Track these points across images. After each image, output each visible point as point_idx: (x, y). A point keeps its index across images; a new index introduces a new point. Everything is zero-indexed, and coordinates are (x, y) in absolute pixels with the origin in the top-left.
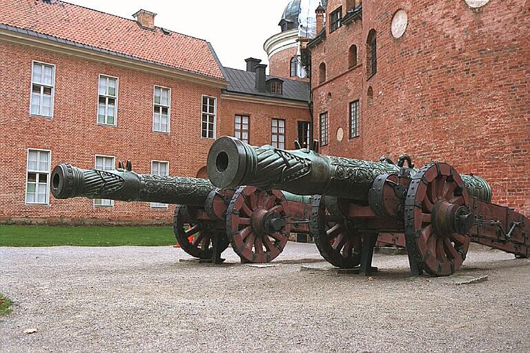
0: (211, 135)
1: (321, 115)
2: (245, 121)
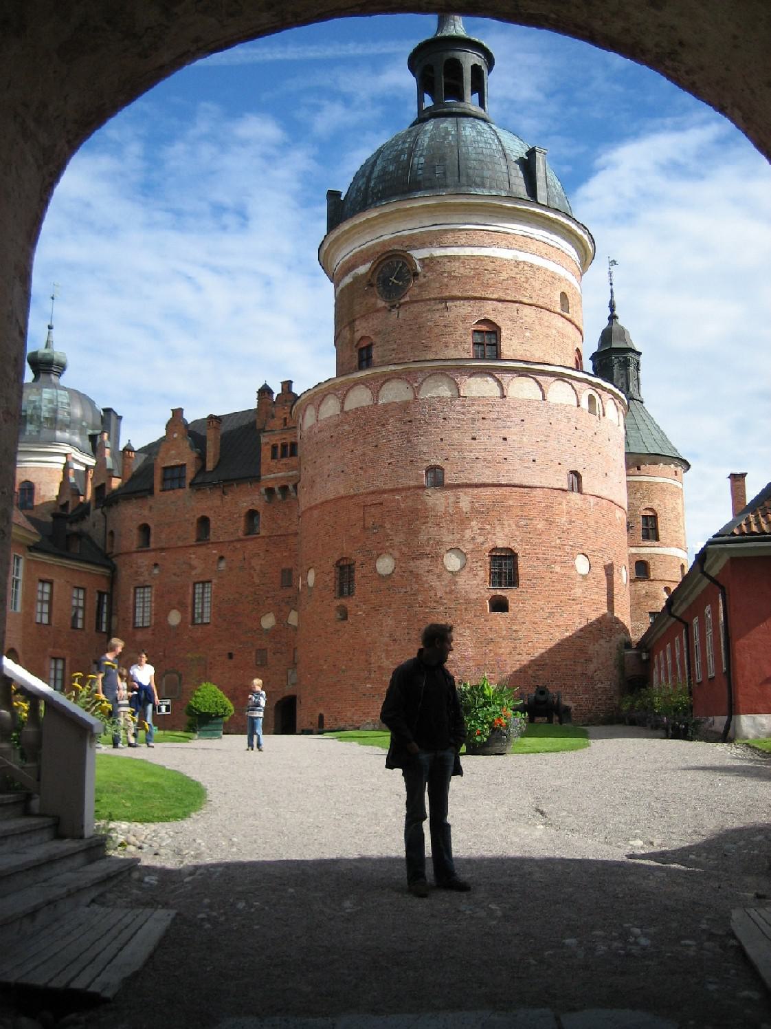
0: (15, 609)
1: (136, 588)
2: (47, 588)
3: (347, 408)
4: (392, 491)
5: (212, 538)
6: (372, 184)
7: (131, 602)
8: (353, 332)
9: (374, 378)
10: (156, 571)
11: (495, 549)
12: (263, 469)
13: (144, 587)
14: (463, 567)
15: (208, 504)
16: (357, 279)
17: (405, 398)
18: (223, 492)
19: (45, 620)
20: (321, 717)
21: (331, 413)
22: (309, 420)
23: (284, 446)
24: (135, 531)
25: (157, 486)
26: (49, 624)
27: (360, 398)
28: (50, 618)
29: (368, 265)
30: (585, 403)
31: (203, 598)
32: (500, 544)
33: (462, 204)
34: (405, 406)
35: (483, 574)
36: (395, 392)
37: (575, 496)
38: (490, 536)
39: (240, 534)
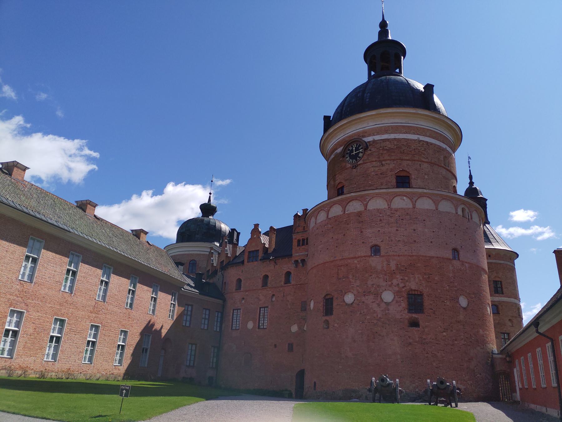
1: (233, 310)
3: (329, 217)
4: (353, 258)
5: (269, 285)
6: (344, 109)
7: (231, 317)
8: (335, 181)
9: (342, 200)
10: (243, 302)
11: (412, 290)
12: (293, 251)
13: (237, 310)
14: (393, 300)
15: (268, 268)
16: (337, 155)
17: (359, 210)
18: (275, 263)
19: (188, 324)
20: (315, 383)
21: (322, 219)
22: (312, 224)
23: (303, 240)
24: (235, 282)
25: (246, 261)
26: (189, 326)
27: (336, 211)
28: (190, 324)
29: (342, 148)
30: (460, 212)
31: (264, 315)
32: (413, 287)
33: (390, 113)
34: (359, 214)
35: (404, 304)
36: (355, 207)
37: (456, 263)
38: (407, 283)
39: (282, 283)
